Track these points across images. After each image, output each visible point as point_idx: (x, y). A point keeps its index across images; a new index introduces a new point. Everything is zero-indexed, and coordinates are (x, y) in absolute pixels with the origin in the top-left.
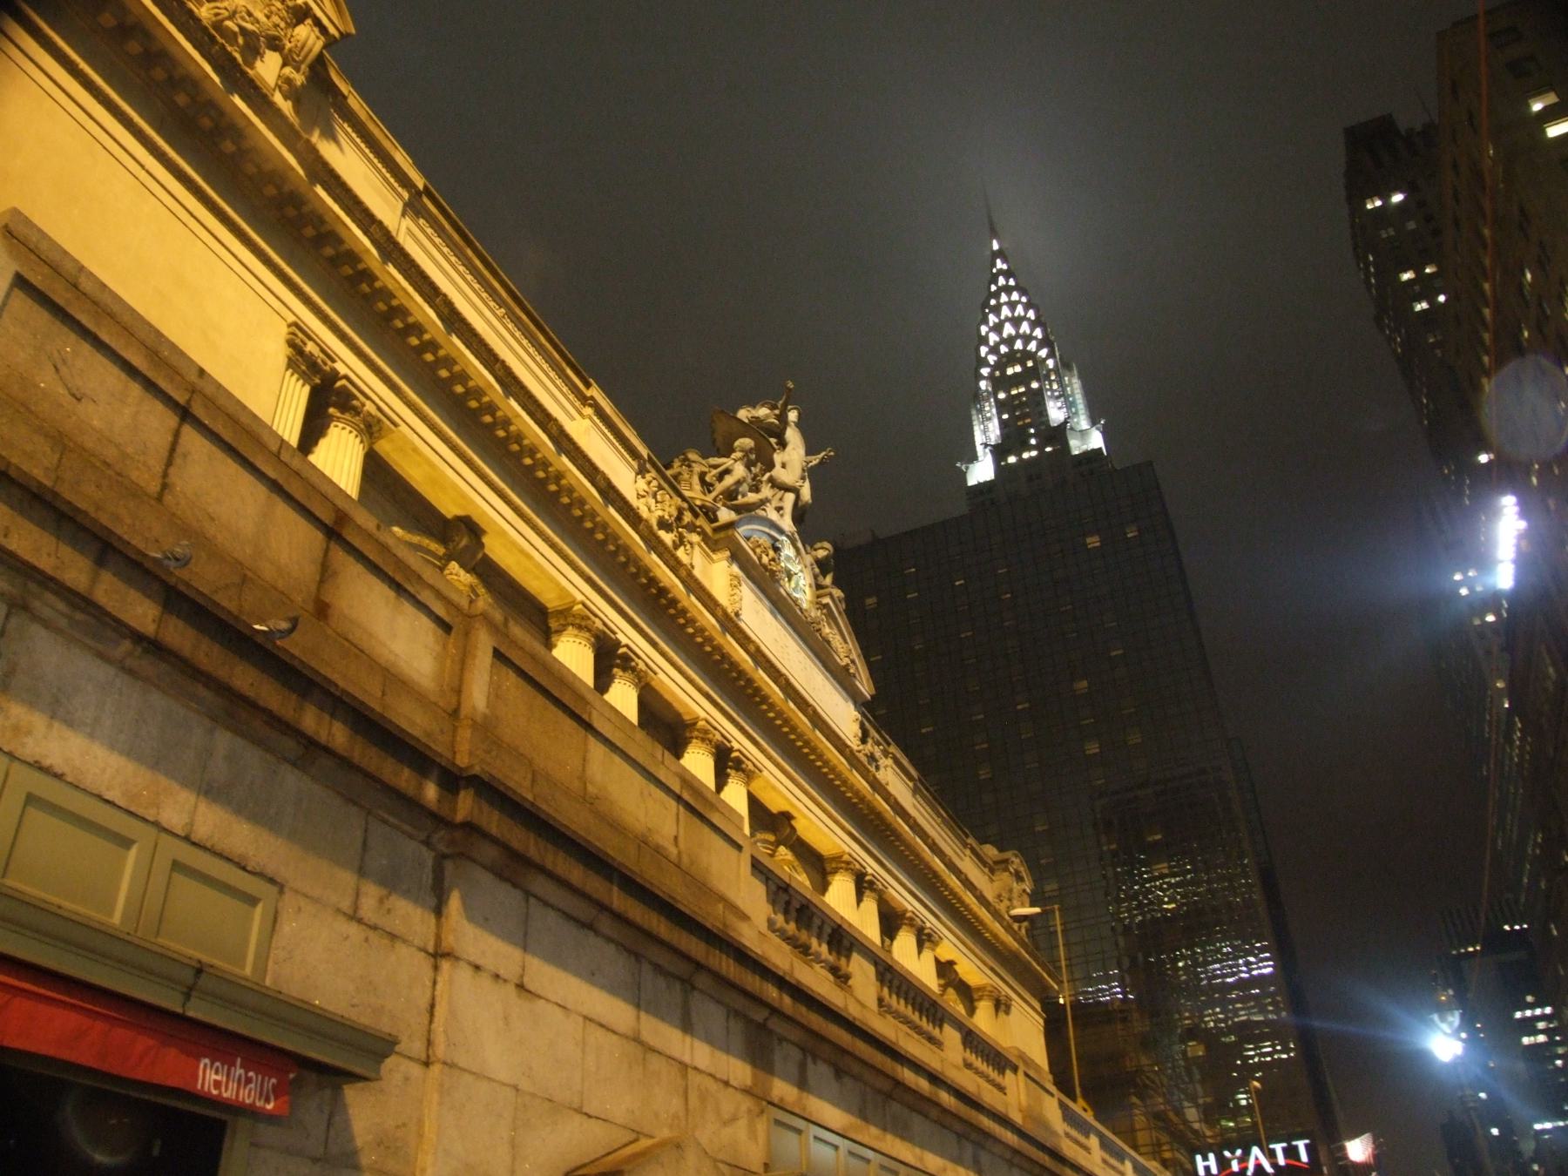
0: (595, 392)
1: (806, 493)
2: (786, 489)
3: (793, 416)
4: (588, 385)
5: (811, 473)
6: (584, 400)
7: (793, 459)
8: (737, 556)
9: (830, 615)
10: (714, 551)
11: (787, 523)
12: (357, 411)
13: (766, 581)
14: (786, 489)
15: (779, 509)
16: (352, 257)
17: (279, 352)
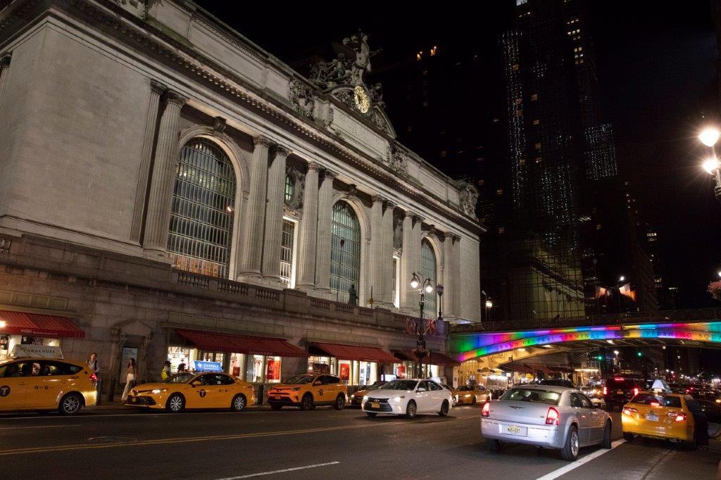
0: (272, 58)
1: (369, 67)
2: (360, 68)
3: (365, 38)
4: (267, 57)
5: (372, 59)
6: (267, 62)
7: (362, 58)
8: (332, 101)
9: (378, 112)
10: (325, 100)
11: (360, 81)
12: (176, 98)
13: (348, 107)
14: (360, 68)
15: (358, 75)
16: (169, 52)
17: (147, 89)
